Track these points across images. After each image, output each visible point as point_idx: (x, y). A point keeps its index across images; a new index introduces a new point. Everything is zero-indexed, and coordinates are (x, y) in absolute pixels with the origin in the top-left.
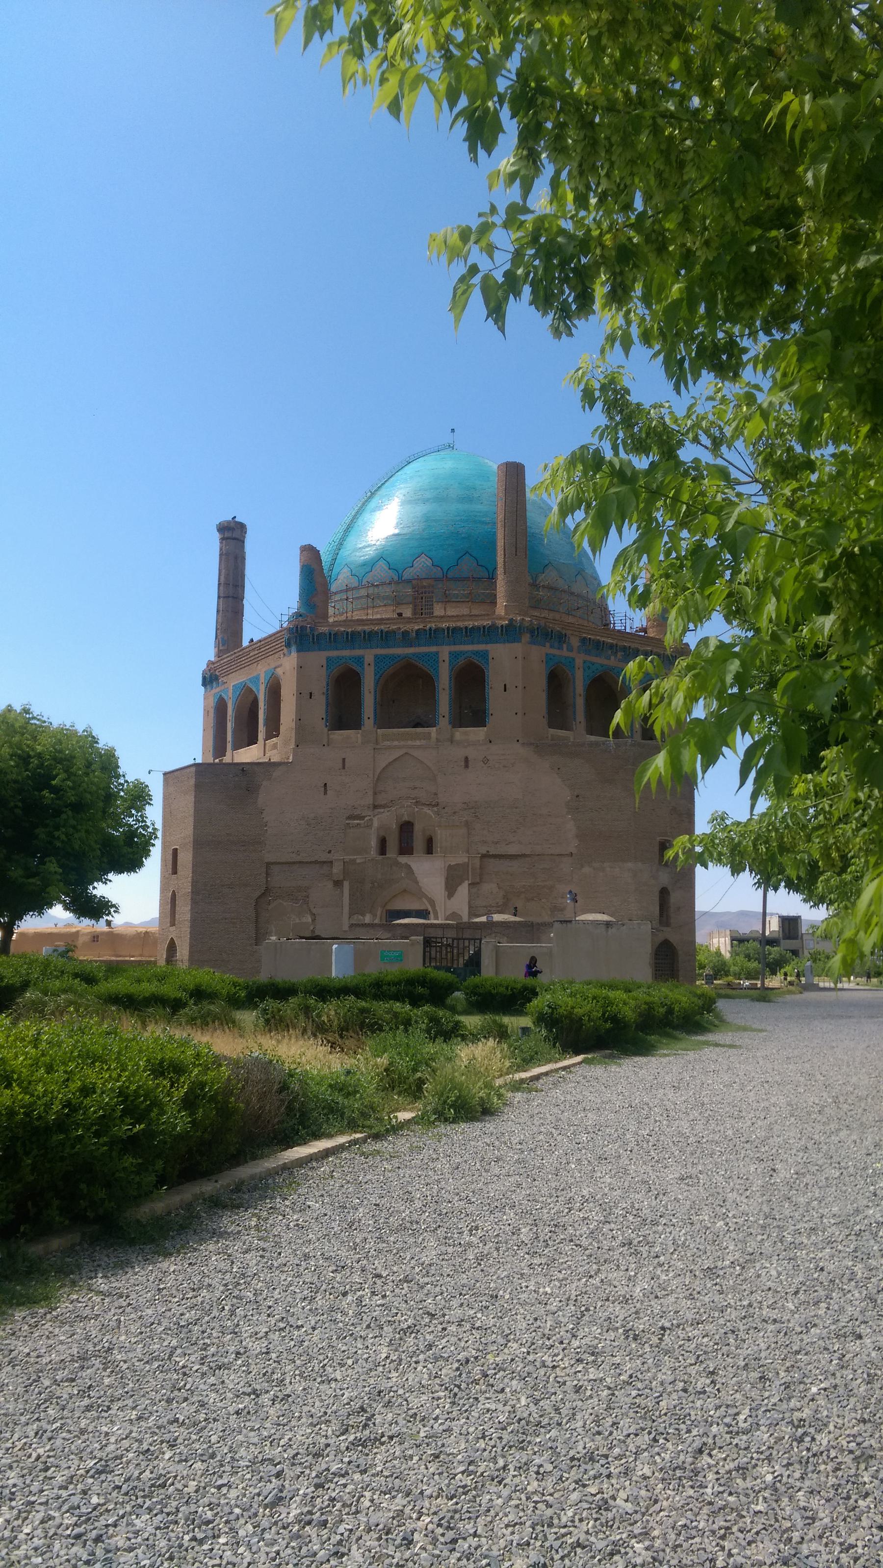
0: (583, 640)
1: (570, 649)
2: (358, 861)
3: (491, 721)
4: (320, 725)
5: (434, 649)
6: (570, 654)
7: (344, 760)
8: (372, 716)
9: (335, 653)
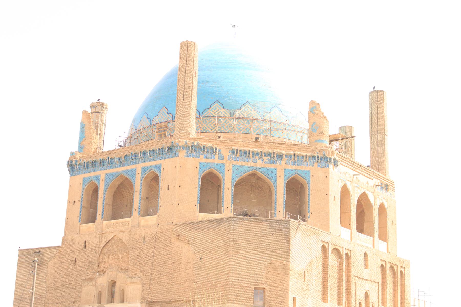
0: (233, 151)
1: (221, 158)
3: (161, 210)
4: (76, 220)
5: (134, 166)
6: (221, 161)
7: (85, 242)
8: (101, 214)
9: (86, 175)
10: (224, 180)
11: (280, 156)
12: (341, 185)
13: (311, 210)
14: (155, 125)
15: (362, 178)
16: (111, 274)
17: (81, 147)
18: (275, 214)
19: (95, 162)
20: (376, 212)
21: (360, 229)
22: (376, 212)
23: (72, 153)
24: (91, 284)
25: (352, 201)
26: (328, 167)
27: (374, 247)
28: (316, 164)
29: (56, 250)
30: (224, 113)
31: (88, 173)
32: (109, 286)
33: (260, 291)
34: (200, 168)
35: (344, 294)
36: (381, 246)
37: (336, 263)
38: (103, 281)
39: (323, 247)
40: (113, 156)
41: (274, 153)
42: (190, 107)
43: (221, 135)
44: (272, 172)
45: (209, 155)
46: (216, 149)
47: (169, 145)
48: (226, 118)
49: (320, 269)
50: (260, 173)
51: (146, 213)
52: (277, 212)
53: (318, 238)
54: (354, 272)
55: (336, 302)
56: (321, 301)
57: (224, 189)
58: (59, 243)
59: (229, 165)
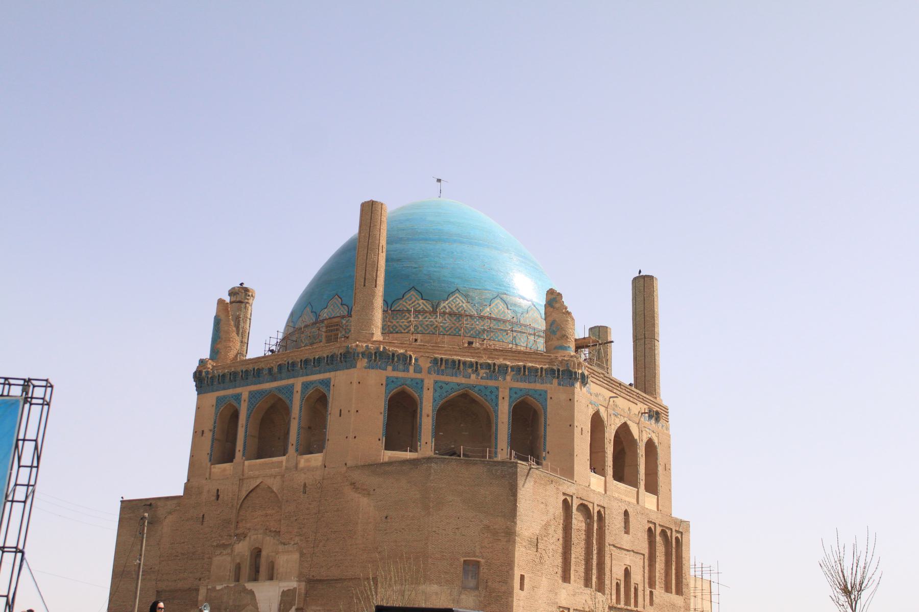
1: (418, 370)
2: (218, 587)
3: (329, 445)
5: (291, 381)
6: (419, 376)
9: (222, 393)
10: (421, 403)
11: (504, 369)
12: (591, 412)
13: (548, 449)
14: (322, 321)
15: (620, 402)
16: (255, 538)
17: (215, 351)
18: (496, 453)
19: (235, 374)
20: (641, 451)
21: (619, 476)
22: (641, 451)
23: (202, 361)
24: (225, 552)
25: (606, 435)
26: (573, 385)
27: (638, 502)
28: (555, 381)
29: (175, 502)
30: (422, 304)
31: (224, 389)
32: (251, 555)
33: (471, 567)
34: (387, 385)
35: (594, 571)
36: (649, 501)
37: (583, 526)
38: (242, 548)
39: (565, 501)
40: (262, 365)
41: (494, 364)
42: (373, 295)
43: (419, 337)
44: (491, 392)
45: (401, 367)
46: (411, 357)
47: (342, 351)
48: (426, 312)
49: (560, 533)
50: (474, 394)
51: (307, 449)
52: (499, 450)
53: (558, 489)
54: (609, 539)
55: (582, 582)
56: (560, 581)
57: (421, 415)
58: (180, 492)
59: (429, 382)
